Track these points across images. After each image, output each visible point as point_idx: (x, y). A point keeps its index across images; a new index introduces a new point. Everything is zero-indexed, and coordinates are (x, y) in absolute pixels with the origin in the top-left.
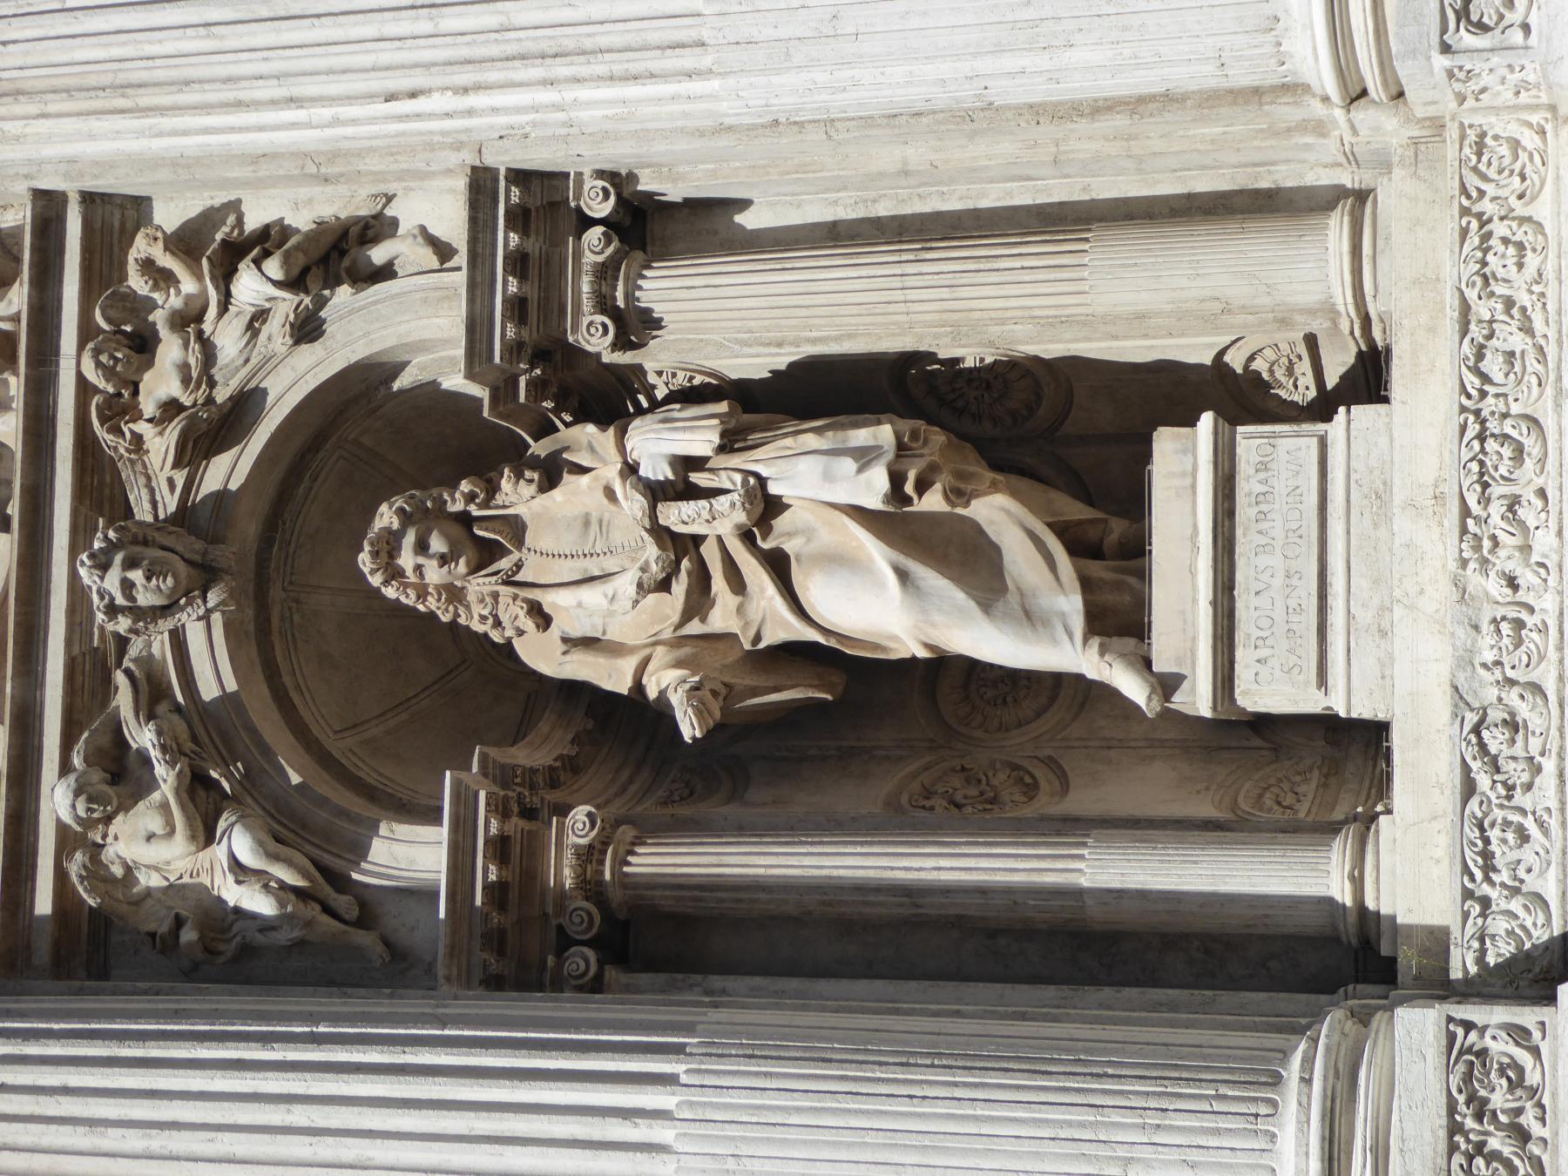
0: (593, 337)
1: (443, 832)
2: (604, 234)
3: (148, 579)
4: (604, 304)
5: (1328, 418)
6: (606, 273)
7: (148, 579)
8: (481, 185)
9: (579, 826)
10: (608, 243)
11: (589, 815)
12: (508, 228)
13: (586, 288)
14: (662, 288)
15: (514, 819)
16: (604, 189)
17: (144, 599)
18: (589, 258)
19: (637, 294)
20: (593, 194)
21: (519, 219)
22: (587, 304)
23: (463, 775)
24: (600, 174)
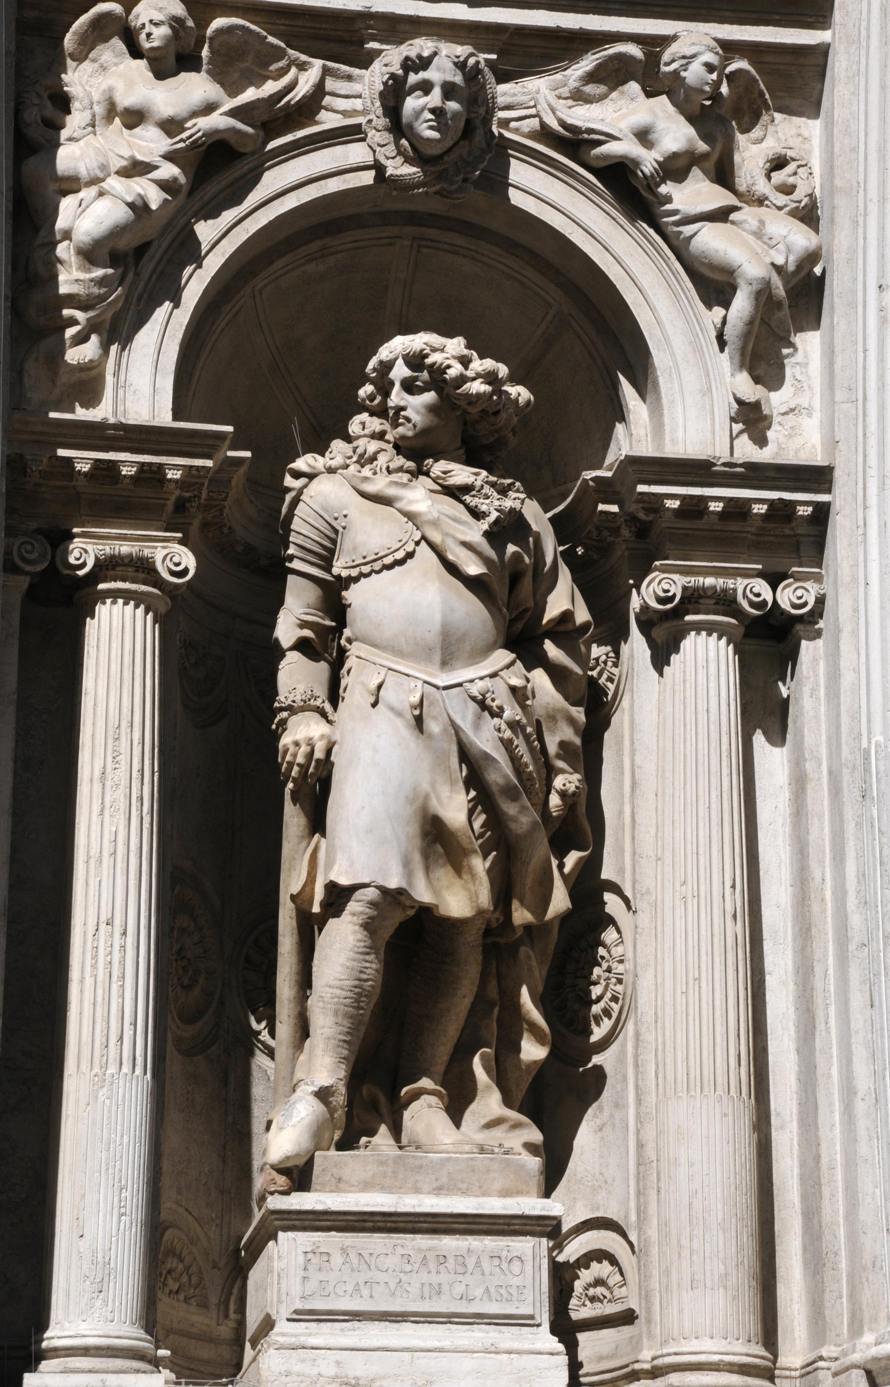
0: (658, 586)
1: (164, 417)
2: (765, 602)
3: (433, 111)
4: (693, 599)
5: (553, 1331)
6: (725, 602)
7: (433, 111)
8: (818, 477)
9: (175, 557)
10: (752, 604)
11: (185, 571)
12: (771, 503)
13: (709, 581)
14: (709, 658)
15: (177, 492)
16: (805, 604)
17: (412, 103)
18: (740, 584)
19: (704, 633)
20: (799, 593)
21: (781, 512)
22: (693, 581)
23: (227, 443)
24: (821, 601)
